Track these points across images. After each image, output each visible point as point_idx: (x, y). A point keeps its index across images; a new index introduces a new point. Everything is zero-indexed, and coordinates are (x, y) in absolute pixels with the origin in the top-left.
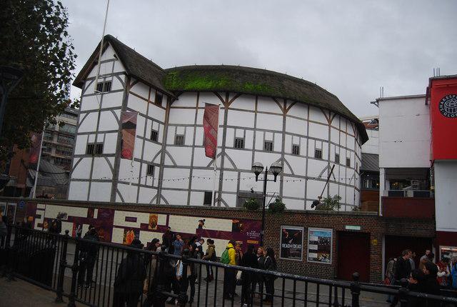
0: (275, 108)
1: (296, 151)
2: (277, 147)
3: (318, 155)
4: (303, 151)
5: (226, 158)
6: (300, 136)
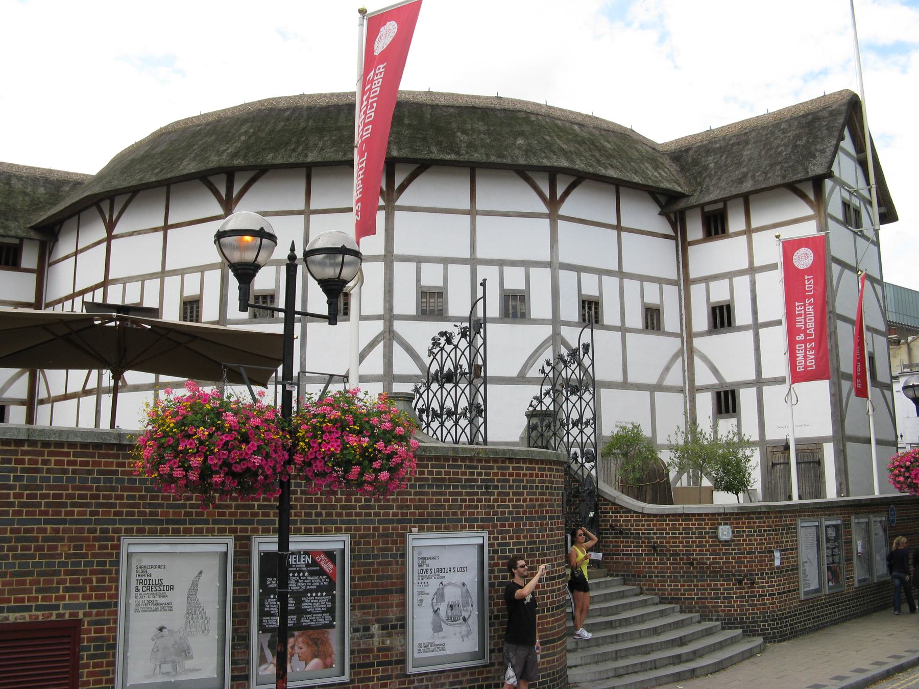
2: (540, 306)
3: (653, 318)
4: (610, 315)
5: (396, 347)
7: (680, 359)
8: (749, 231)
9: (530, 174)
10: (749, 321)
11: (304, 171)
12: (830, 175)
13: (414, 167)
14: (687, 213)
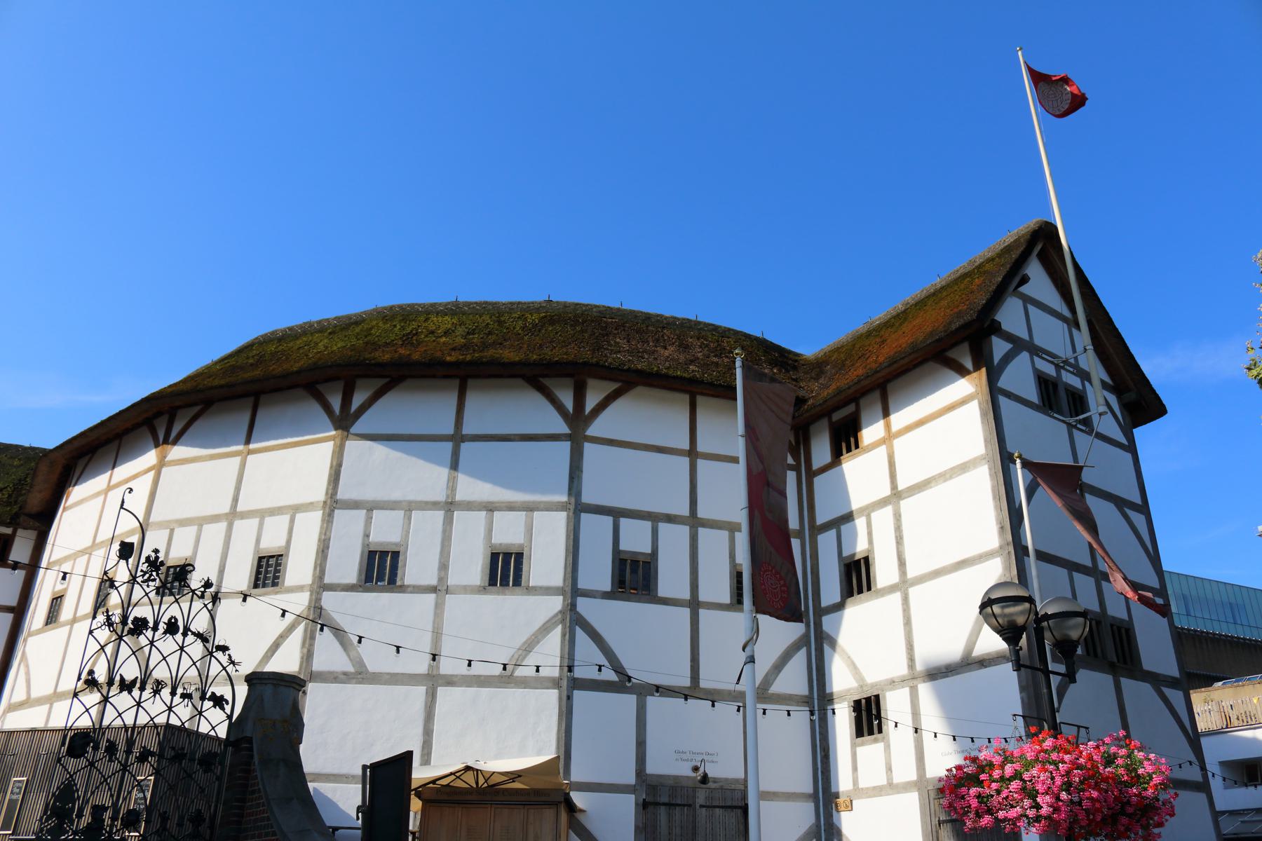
0: (531, 411)
1: (634, 577)
4: (671, 580)
6: (655, 518)
7: (803, 651)
8: (889, 438)
9: (547, 382)
10: (894, 578)
11: (251, 399)
12: (996, 329)
13: (380, 382)
14: (812, 428)
